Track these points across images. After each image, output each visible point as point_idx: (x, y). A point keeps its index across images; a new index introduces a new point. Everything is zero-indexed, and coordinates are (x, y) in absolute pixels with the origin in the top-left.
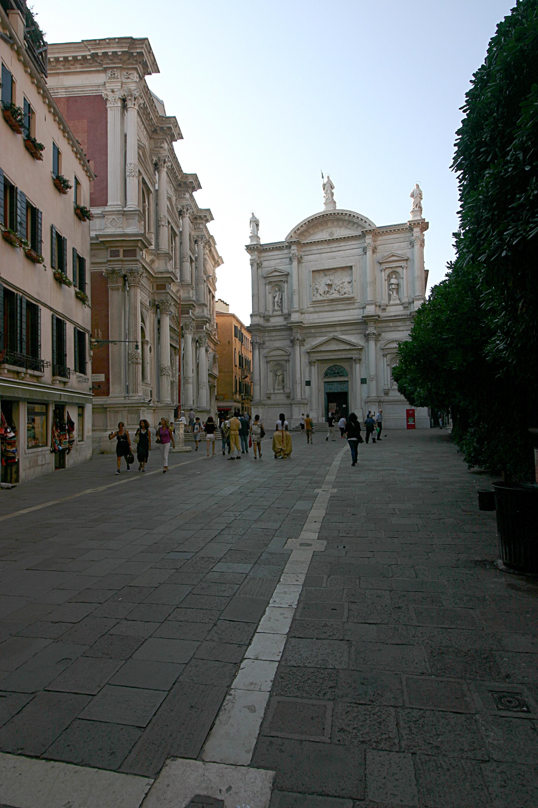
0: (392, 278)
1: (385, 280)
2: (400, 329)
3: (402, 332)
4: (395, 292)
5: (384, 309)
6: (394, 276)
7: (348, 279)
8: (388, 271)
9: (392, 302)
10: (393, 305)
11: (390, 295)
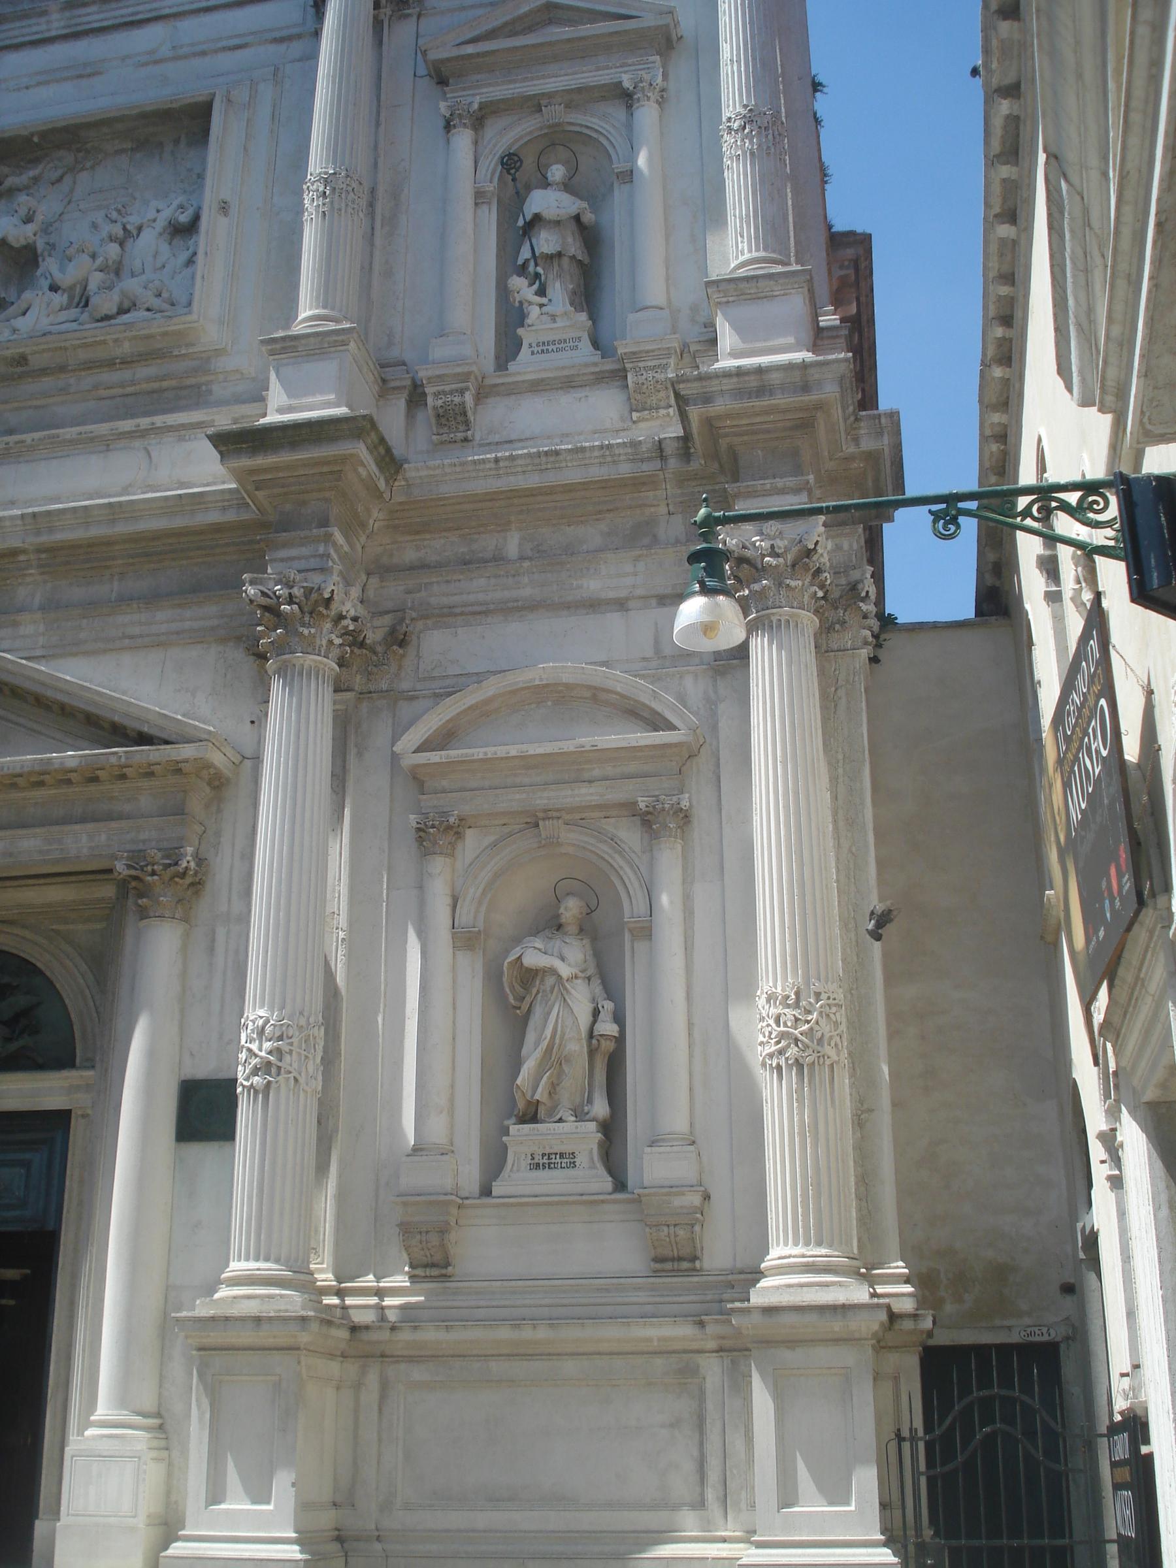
0: (545, 184)
1: (479, 197)
2: (593, 586)
3: (614, 620)
4: (559, 292)
5: (454, 422)
6: (557, 172)
7: (167, 210)
8: (506, 135)
9: (526, 365)
10: (537, 387)
11: (511, 320)
